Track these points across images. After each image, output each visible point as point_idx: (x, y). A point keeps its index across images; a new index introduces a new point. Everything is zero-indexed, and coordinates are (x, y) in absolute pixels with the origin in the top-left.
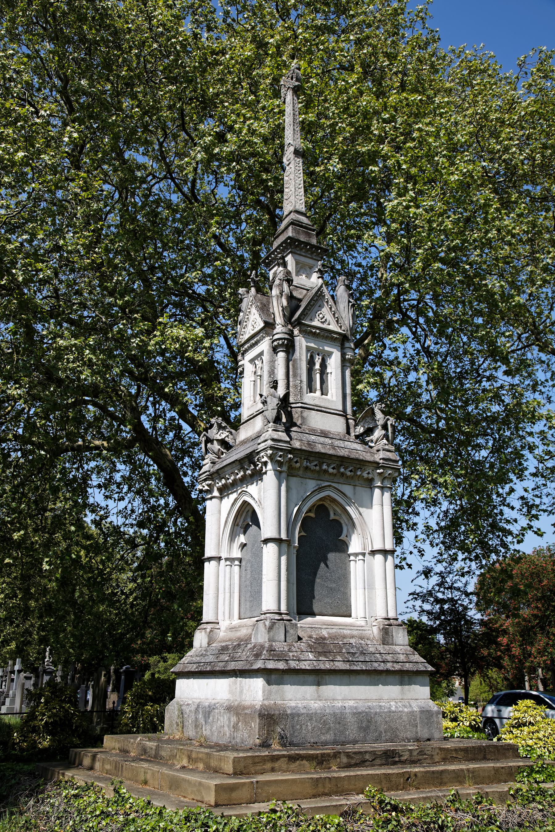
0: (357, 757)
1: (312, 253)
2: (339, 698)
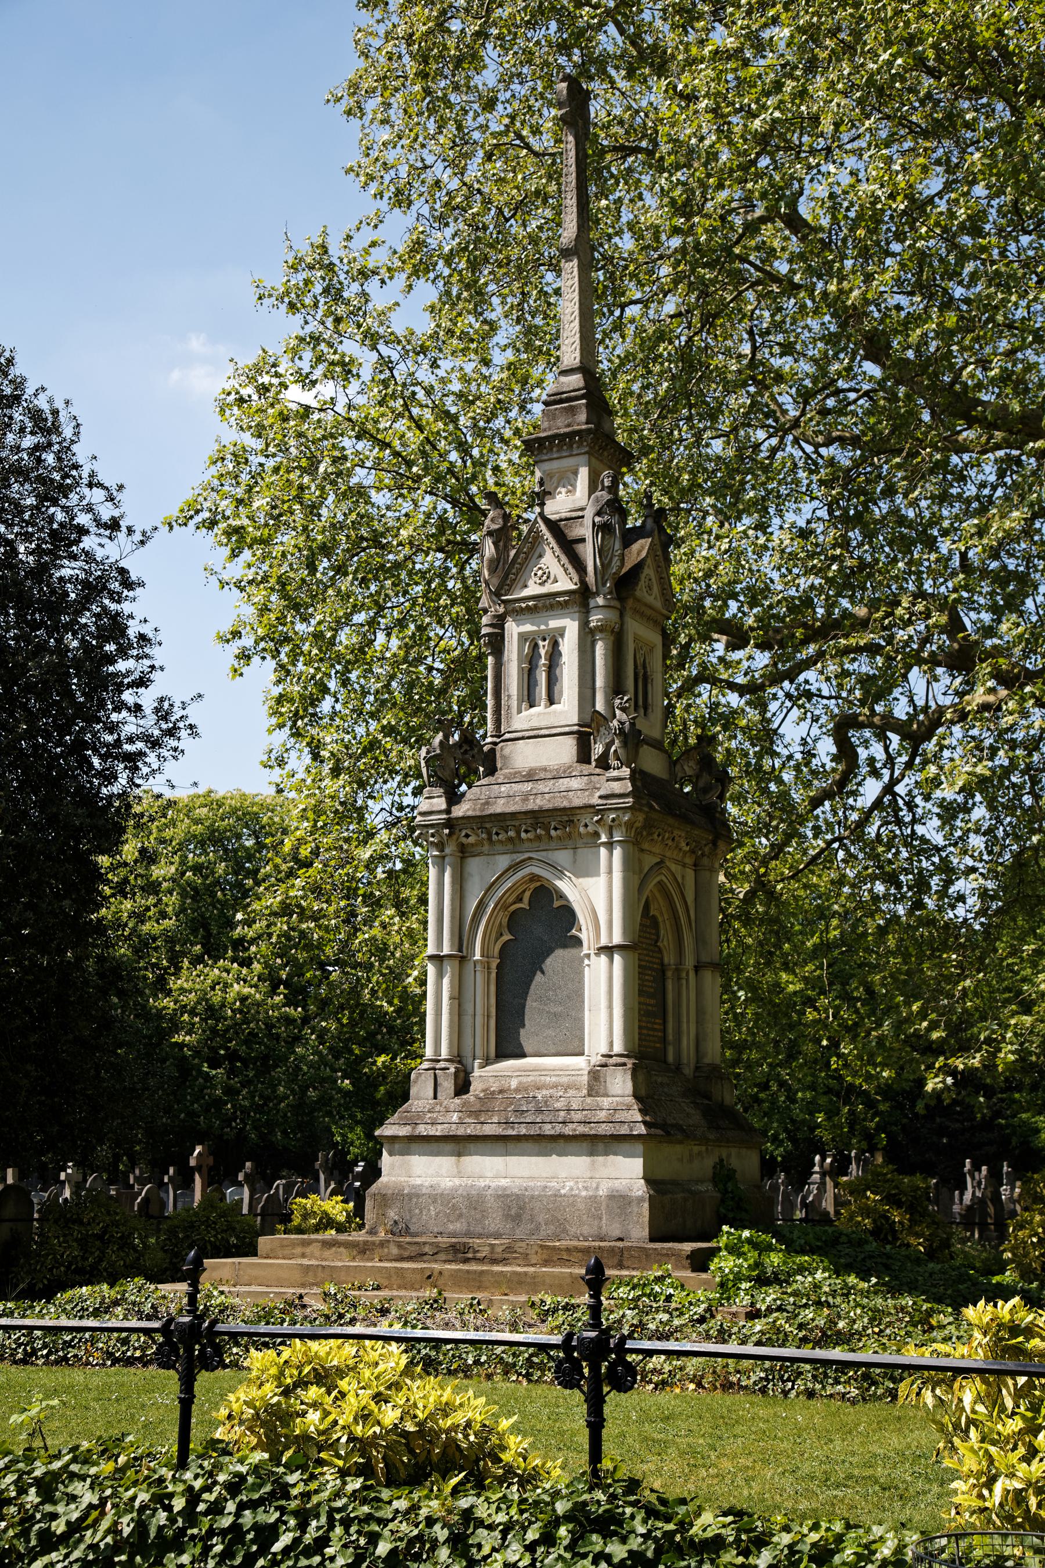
1: (571, 447)
2: (489, 1174)
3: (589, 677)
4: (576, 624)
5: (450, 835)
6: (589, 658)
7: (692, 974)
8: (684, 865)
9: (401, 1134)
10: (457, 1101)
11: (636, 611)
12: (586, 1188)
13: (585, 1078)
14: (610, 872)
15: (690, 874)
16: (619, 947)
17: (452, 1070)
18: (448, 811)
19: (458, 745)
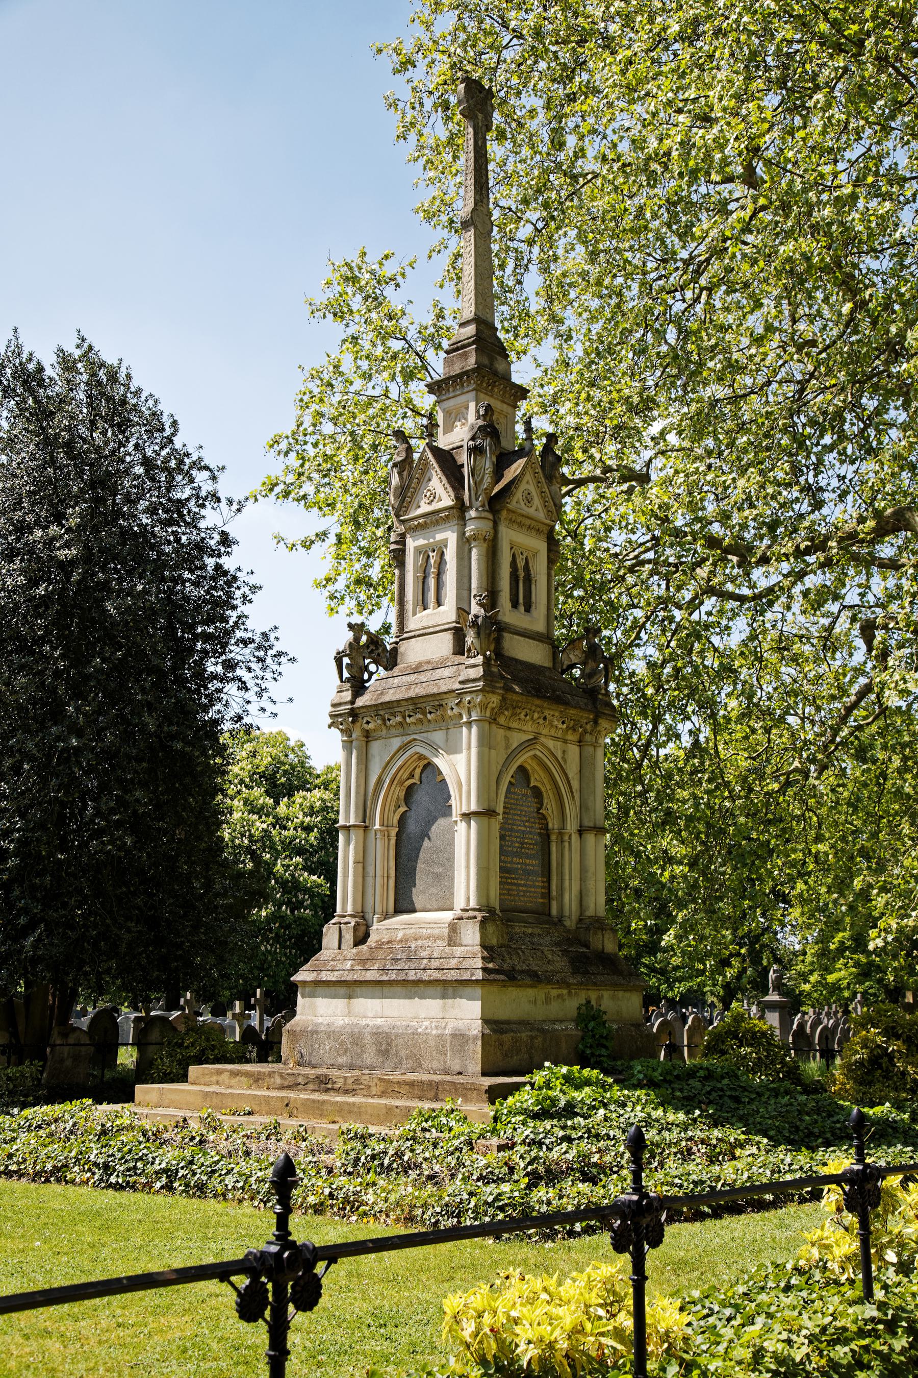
0: (291, 1079)
3: (466, 580)
4: (455, 535)
5: (353, 722)
6: (466, 563)
7: (575, 838)
8: (565, 741)
9: (308, 979)
10: (354, 950)
11: (513, 522)
12: (437, 1027)
13: (446, 930)
14: (469, 748)
15: (573, 751)
16: (475, 814)
17: (353, 924)
18: (352, 702)
19: (367, 646)
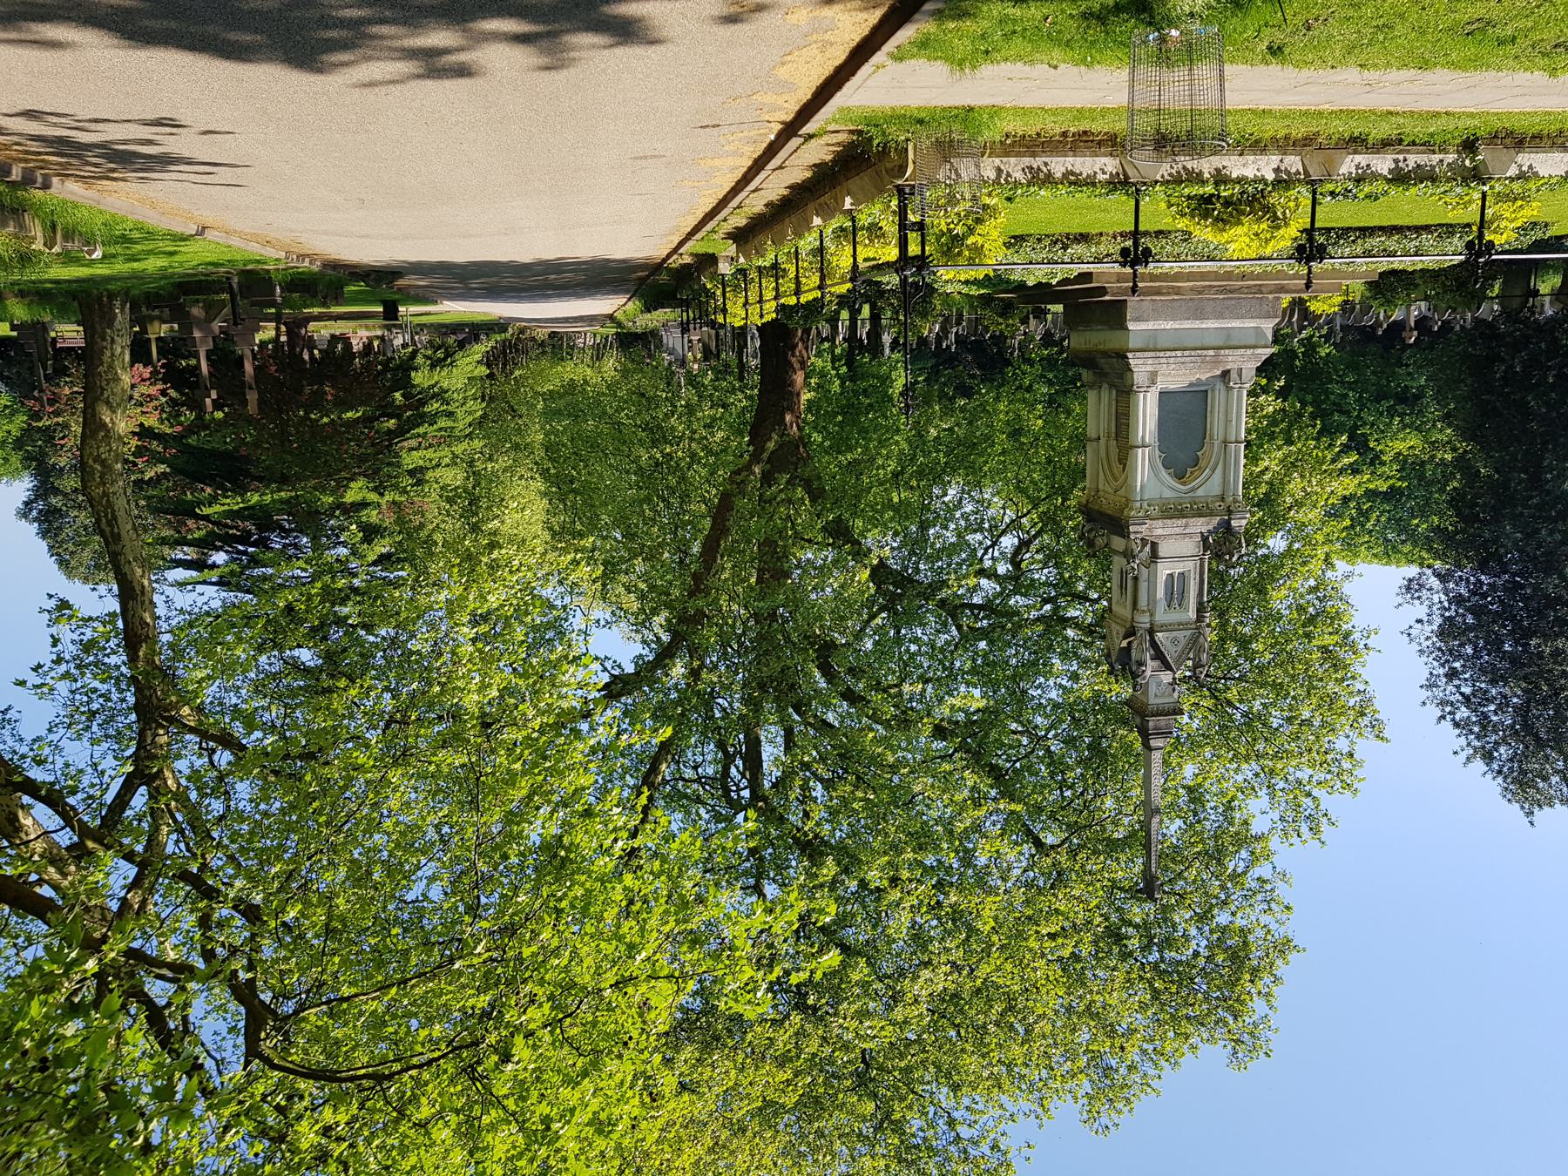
15: (1101, 487)
